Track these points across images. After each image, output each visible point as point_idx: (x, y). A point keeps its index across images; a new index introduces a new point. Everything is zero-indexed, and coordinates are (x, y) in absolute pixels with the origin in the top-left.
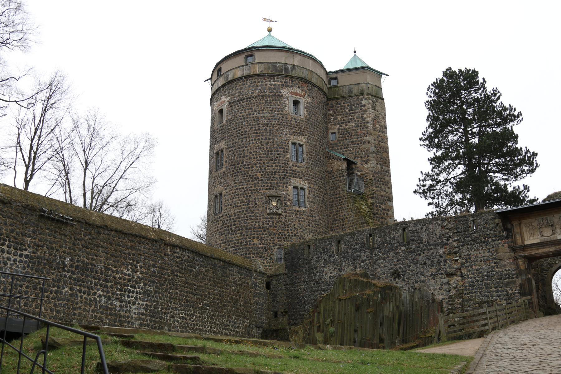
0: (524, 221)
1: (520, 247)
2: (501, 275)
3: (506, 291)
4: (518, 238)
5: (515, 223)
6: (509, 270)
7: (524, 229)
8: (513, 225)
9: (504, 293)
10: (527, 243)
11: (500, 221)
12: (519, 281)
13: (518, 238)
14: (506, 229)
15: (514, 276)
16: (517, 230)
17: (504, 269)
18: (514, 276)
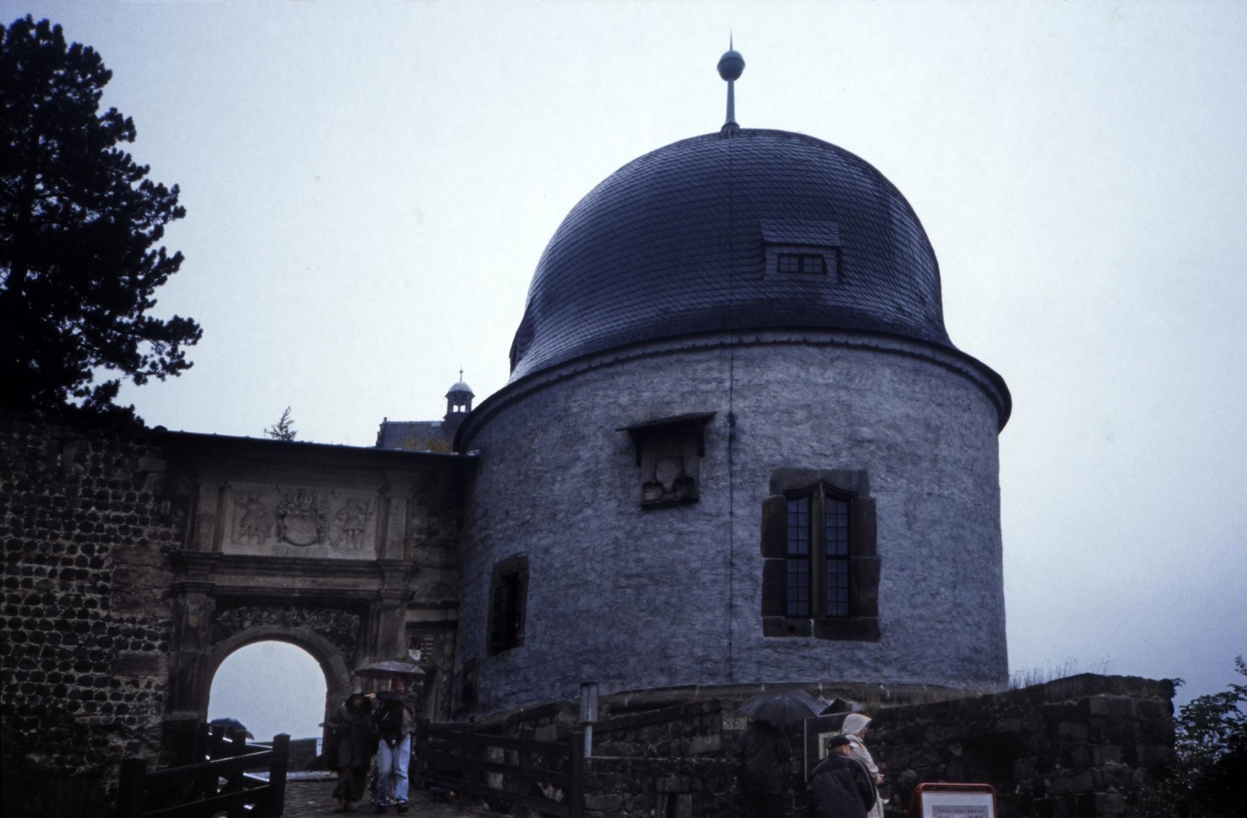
1: (207, 556)
2: (113, 631)
3: (116, 684)
4: (205, 530)
6: (144, 621)
7: (230, 506)
9: (107, 690)
10: (228, 549)
13: (203, 531)
15: (157, 643)
17: (126, 616)
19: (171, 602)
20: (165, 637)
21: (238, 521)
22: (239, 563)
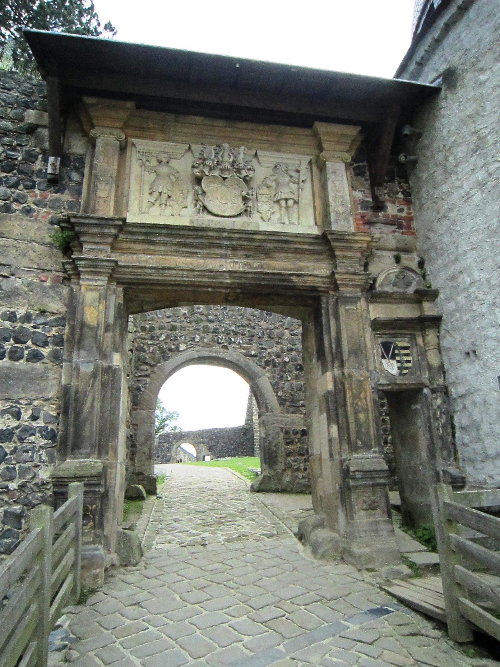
0: (141, 144)
1: (103, 222)
5: (106, 138)
8: (92, 143)
11: (46, 119)
12: (55, 379)
14: (58, 149)
15: (45, 351)
16: (105, 162)
18: (45, 351)
19: (65, 291)
20: (59, 341)
21: (146, 188)
22: (150, 233)
